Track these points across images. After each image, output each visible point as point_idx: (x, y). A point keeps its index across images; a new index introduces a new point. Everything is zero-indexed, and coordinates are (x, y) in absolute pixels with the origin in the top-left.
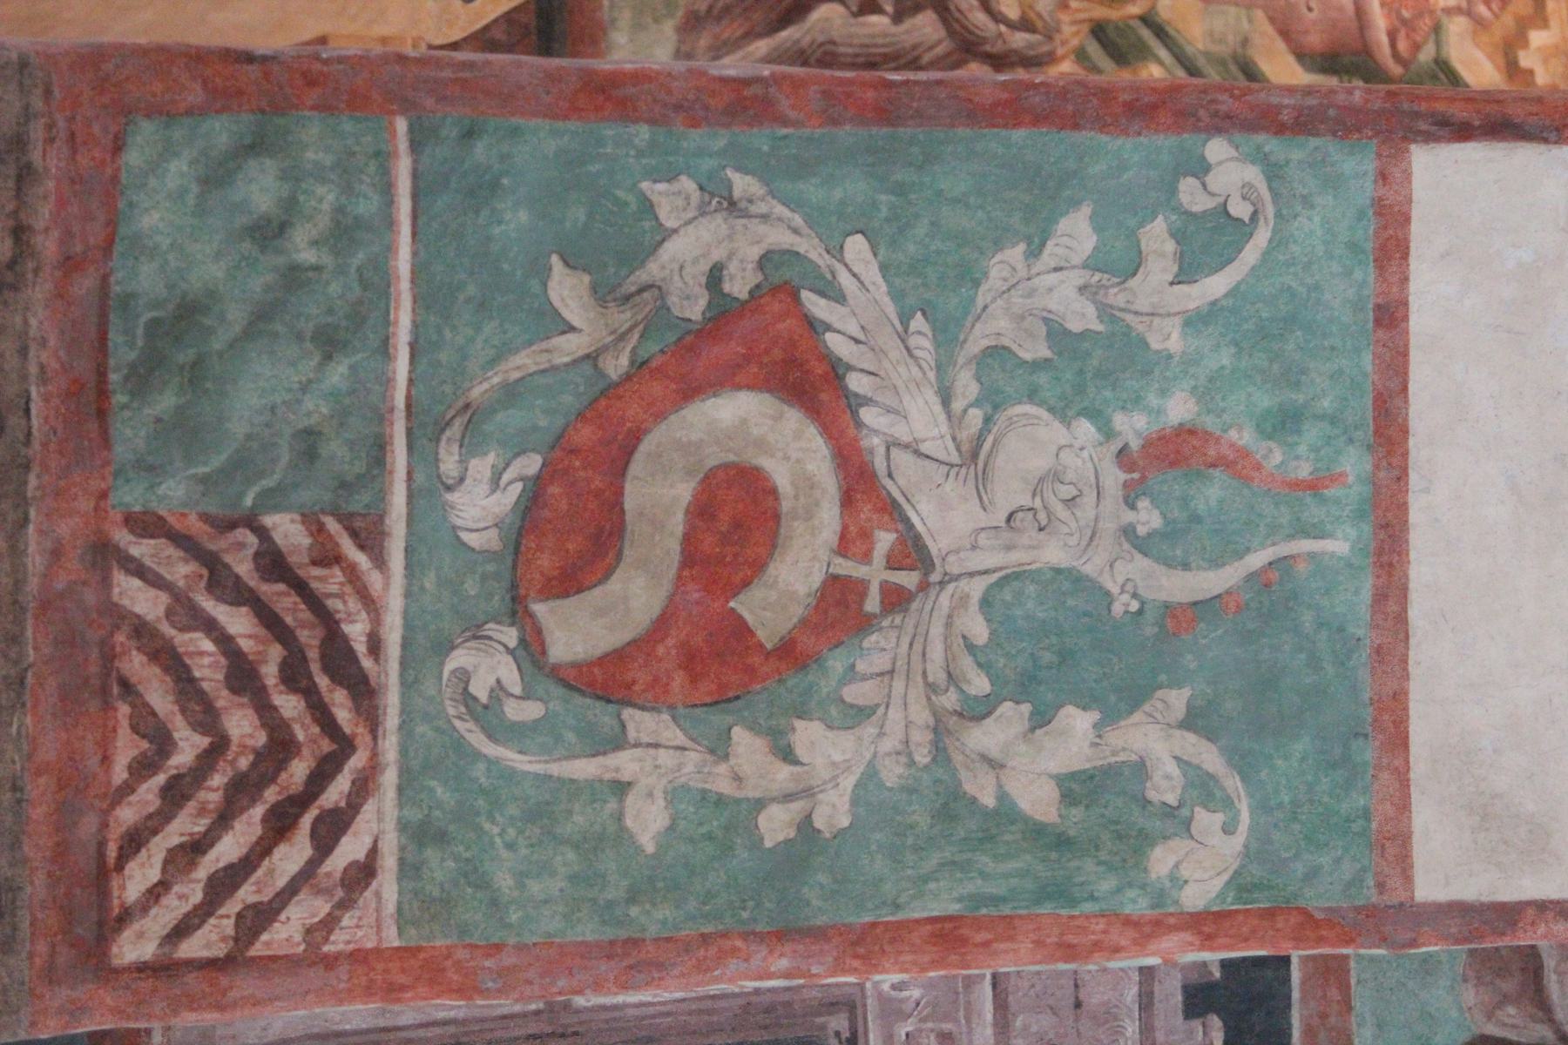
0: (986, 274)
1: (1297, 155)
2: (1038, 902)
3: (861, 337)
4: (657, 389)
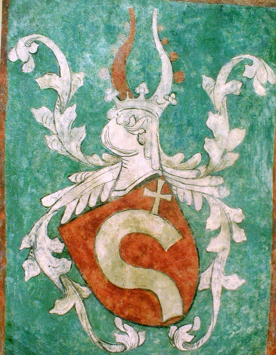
0: (56, 151)
1: (15, 24)
2: (271, 140)
3: (77, 200)
4: (94, 277)
